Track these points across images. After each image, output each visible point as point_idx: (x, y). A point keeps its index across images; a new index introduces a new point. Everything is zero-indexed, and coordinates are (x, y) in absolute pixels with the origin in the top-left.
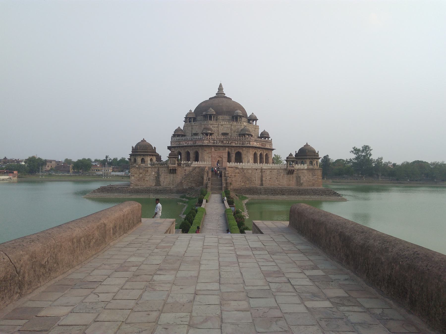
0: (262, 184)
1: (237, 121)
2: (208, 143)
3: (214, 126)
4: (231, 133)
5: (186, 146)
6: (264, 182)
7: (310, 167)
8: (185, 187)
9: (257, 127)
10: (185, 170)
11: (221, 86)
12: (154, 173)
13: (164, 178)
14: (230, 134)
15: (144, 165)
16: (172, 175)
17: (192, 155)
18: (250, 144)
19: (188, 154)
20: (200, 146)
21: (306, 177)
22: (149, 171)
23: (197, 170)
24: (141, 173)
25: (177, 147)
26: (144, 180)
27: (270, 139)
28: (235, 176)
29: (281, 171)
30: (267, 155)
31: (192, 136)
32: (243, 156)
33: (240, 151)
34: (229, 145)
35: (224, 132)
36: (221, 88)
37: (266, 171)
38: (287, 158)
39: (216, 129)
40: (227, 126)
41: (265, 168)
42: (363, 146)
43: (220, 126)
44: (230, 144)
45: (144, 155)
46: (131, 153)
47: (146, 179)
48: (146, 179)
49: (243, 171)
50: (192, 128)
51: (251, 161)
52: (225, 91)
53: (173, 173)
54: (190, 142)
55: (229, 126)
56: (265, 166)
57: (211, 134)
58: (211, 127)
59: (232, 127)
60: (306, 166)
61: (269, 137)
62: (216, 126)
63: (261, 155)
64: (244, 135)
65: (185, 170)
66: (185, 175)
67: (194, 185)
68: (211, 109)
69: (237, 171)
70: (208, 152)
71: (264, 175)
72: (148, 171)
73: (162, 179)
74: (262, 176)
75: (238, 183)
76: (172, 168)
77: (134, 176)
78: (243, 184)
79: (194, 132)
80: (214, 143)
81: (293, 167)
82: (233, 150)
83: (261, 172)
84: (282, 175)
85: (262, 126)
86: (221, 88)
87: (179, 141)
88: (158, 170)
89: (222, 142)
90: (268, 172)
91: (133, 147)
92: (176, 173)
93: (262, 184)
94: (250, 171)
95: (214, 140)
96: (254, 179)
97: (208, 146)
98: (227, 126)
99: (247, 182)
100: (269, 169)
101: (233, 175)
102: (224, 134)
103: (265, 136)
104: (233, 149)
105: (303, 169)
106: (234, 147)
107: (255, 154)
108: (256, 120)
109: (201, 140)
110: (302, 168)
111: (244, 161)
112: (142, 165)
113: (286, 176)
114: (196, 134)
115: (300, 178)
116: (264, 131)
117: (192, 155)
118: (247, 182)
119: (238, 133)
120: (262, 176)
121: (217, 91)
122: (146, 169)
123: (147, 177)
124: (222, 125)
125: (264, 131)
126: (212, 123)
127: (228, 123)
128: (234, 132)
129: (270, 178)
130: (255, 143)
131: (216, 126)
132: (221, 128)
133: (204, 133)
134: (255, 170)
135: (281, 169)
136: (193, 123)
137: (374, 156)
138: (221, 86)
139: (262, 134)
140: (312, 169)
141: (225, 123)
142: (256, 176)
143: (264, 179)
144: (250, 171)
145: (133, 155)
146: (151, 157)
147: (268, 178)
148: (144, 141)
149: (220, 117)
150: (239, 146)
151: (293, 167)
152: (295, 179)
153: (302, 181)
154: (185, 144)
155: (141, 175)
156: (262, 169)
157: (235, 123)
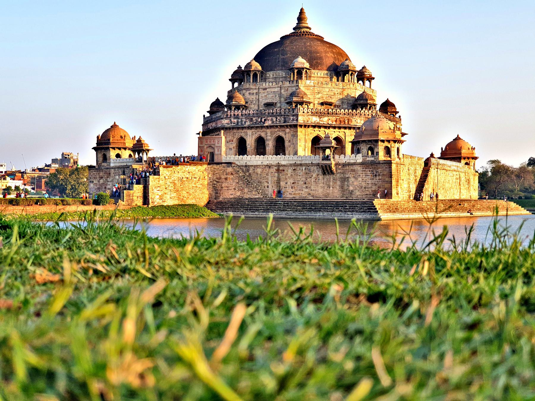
3: (251, 91)
4: (280, 103)
14: (278, 105)
15: (105, 164)
21: (360, 179)
22: (112, 174)
24: (102, 178)
28: (226, 179)
29: (312, 168)
35: (269, 101)
37: (285, 168)
39: (254, 97)
40: (273, 90)
41: (283, 163)
44: (264, 123)
46: (95, 146)
49: (248, 170)
55: (276, 90)
59: (282, 91)
62: (255, 91)
69: (230, 170)
71: (282, 177)
72: (110, 174)
75: (230, 192)
77: (93, 182)
78: (238, 194)
82: (269, 134)
83: (278, 170)
84: (314, 175)
89: (251, 120)
90: (290, 171)
91: (98, 137)
94: (259, 170)
95: (238, 118)
96: (266, 184)
98: (273, 90)
100: (291, 165)
101: (223, 177)
104: (269, 131)
106: (267, 127)
110: (352, 161)
112: (103, 164)
113: (321, 177)
115: (348, 181)
118: (246, 190)
122: (108, 171)
123: (109, 183)
124: (265, 89)
126: (248, 86)
129: (293, 181)
131: (255, 91)
132: (262, 94)
134: (267, 169)
142: (270, 179)
143: (282, 184)
144: (259, 170)
146: (117, 151)
150: (277, 126)
152: (338, 183)
156: (278, 165)
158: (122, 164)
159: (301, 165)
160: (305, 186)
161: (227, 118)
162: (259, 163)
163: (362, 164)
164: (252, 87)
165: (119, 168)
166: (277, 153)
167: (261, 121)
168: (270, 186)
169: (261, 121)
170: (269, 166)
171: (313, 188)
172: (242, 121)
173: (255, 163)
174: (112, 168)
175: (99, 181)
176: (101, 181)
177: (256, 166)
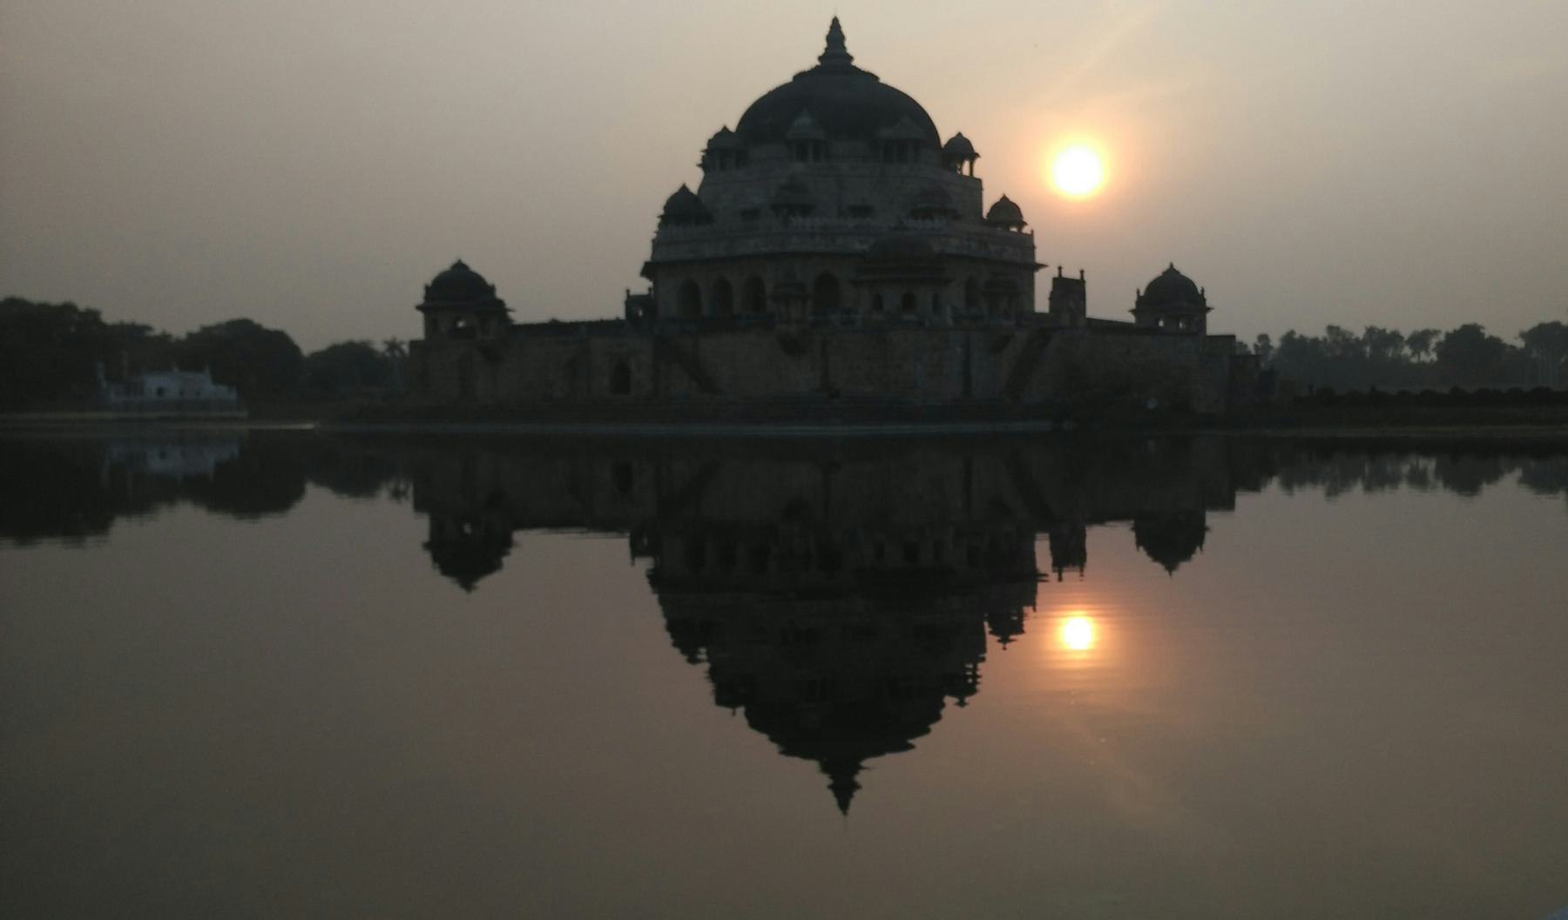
9: (976, 185)
11: (835, 22)
27: (1026, 230)
36: (835, 35)
52: (851, 46)
57: (806, 210)
61: (1022, 224)
86: (835, 35)
108: (973, 156)
121: (820, 46)
138: (835, 22)
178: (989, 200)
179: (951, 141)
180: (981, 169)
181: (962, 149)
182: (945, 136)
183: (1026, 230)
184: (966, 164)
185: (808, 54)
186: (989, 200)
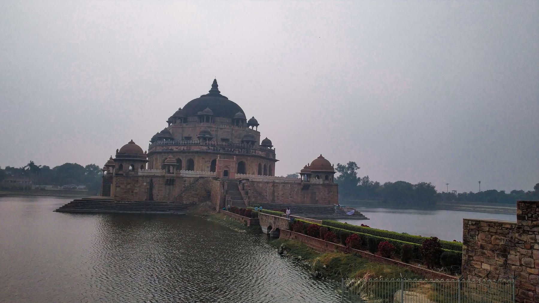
0: (273, 200)
1: (237, 125)
2: (207, 150)
3: (212, 129)
5: (177, 152)
6: (276, 198)
7: (326, 182)
8: (185, 202)
9: (258, 134)
10: (185, 181)
11: (215, 81)
12: (145, 184)
13: (159, 190)
14: (231, 140)
16: (168, 187)
17: (184, 164)
18: (255, 152)
19: (179, 161)
20: (197, 152)
23: (201, 181)
25: (165, 153)
26: (132, 192)
27: (273, 148)
30: (270, 166)
31: (182, 140)
32: (247, 167)
33: (244, 160)
34: (232, 153)
35: (224, 137)
38: (302, 171)
42: (348, 162)
43: (219, 129)
44: (233, 152)
45: (134, 161)
47: (135, 191)
48: (135, 191)
50: (183, 131)
51: (256, 172)
52: (220, 88)
53: (170, 185)
54: (182, 148)
55: (229, 130)
56: (267, 178)
57: (210, 139)
58: (209, 130)
60: (321, 181)
62: (215, 129)
63: (265, 166)
64: (248, 142)
65: (185, 181)
66: (184, 187)
67: (196, 200)
68: (208, 109)
70: (206, 160)
72: (138, 181)
73: (155, 192)
74: (274, 191)
76: (169, 178)
77: (119, 187)
79: (186, 135)
80: (214, 150)
81: (309, 181)
83: (273, 186)
84: (296, 190)
85: (264, 132)
87: (166, 145)
88: (152, 180)
89: (224, 149)
90: (281, 186)
91: (118, 150)
92: (173, 185)
93: (273, 200)
94: (261, 185)
97: (207, 152)
99: (259, 198)
100: (282, 183)
102: (223, 140)
103: (267, 143)
105: (319, 185)
107: (260, 165)
108: (257, 125)
109: (197, 144)
111: (248, 172)
113: (300, 191)
114: (188, 138)
116: (267, 138)
117: (184, 164)
118: (259, 198)
119: (240, 140)
120: (274, 191)
121: (210, 88)
123: (136, 188)
124: (221, 129)
125: (267, 138)
127: (228, 126)
128: (236, 137)
130: (260, 153)
133: (202, 137)
135: (295, 183)
136: (184, 125)
137: (360, 174)
138: (215, 81)
139: (263, 141)
140: (328, 185)
141: (226, 126)
142: (268, 190)
143: (276, 194)
144: (261, 185)
145: (119, 160)
147: (281, 193)
148: (132, 142)
149: (218, 119)
150: (243, 155)
151: (309, 181)
153: (317, 199)
154: (175, 150)
155: (129, 186)
156: (274, 183)
157: (237, 128)
158: (151, 174)
159: (288, 183)
160: (290, 196)
161: (206, 145)
162: (261, 180)
163: (323, 185)
164: (212, 126)
165: (147, 177)
166: (265, 174)
167: (231, 150)
168: (268, 195)
169: (231, 150)
170: (268, 183)
171: (295, 197)
172: (217, 149)
173: (258, 180)
174: (140, 176)
175: (126, 186)
176: (129, 186)
177: (259, 182)
178: (262, 139)
179: (250, 120)
180: (259, 129)
181: (254, 122)
182: (248, 118)
183: (273, 148)
184: (255, 128)
185: (206, 90)
186: (262, 139)
